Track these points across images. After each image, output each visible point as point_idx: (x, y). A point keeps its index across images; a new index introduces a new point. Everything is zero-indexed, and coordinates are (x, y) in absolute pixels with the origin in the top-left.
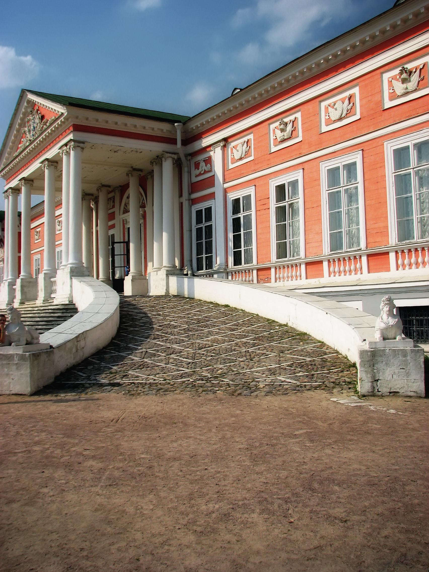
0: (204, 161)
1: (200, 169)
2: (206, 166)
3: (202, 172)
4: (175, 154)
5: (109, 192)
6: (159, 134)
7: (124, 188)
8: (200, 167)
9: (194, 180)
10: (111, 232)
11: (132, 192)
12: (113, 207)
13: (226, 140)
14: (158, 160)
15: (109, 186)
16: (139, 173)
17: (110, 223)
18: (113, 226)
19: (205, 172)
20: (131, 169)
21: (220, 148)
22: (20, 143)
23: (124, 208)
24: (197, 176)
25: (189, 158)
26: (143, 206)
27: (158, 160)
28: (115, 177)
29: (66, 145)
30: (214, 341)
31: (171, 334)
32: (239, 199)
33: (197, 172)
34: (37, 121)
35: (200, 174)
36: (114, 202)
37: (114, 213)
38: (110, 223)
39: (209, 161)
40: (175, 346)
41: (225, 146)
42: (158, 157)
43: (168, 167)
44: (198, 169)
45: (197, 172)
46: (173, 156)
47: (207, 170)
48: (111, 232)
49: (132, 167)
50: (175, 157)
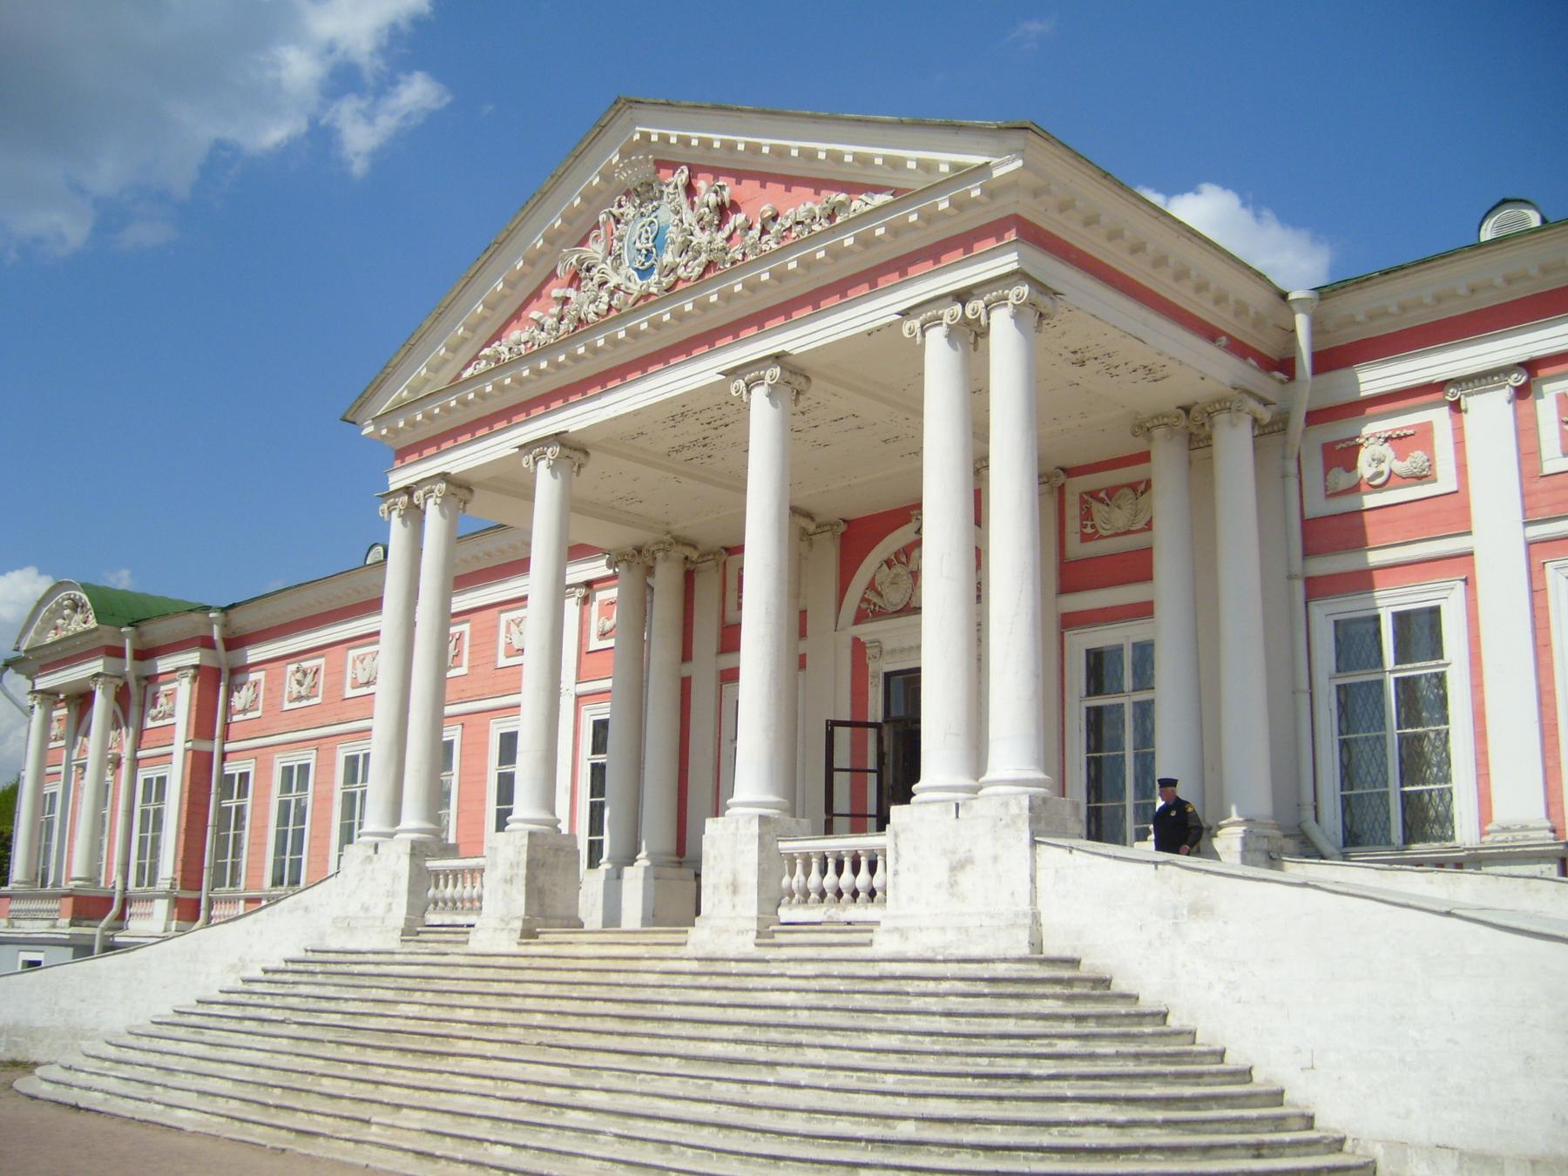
0: (1387, 440)
13: (1531, 366)
21: (1507, 393)
50: (1266, 415)
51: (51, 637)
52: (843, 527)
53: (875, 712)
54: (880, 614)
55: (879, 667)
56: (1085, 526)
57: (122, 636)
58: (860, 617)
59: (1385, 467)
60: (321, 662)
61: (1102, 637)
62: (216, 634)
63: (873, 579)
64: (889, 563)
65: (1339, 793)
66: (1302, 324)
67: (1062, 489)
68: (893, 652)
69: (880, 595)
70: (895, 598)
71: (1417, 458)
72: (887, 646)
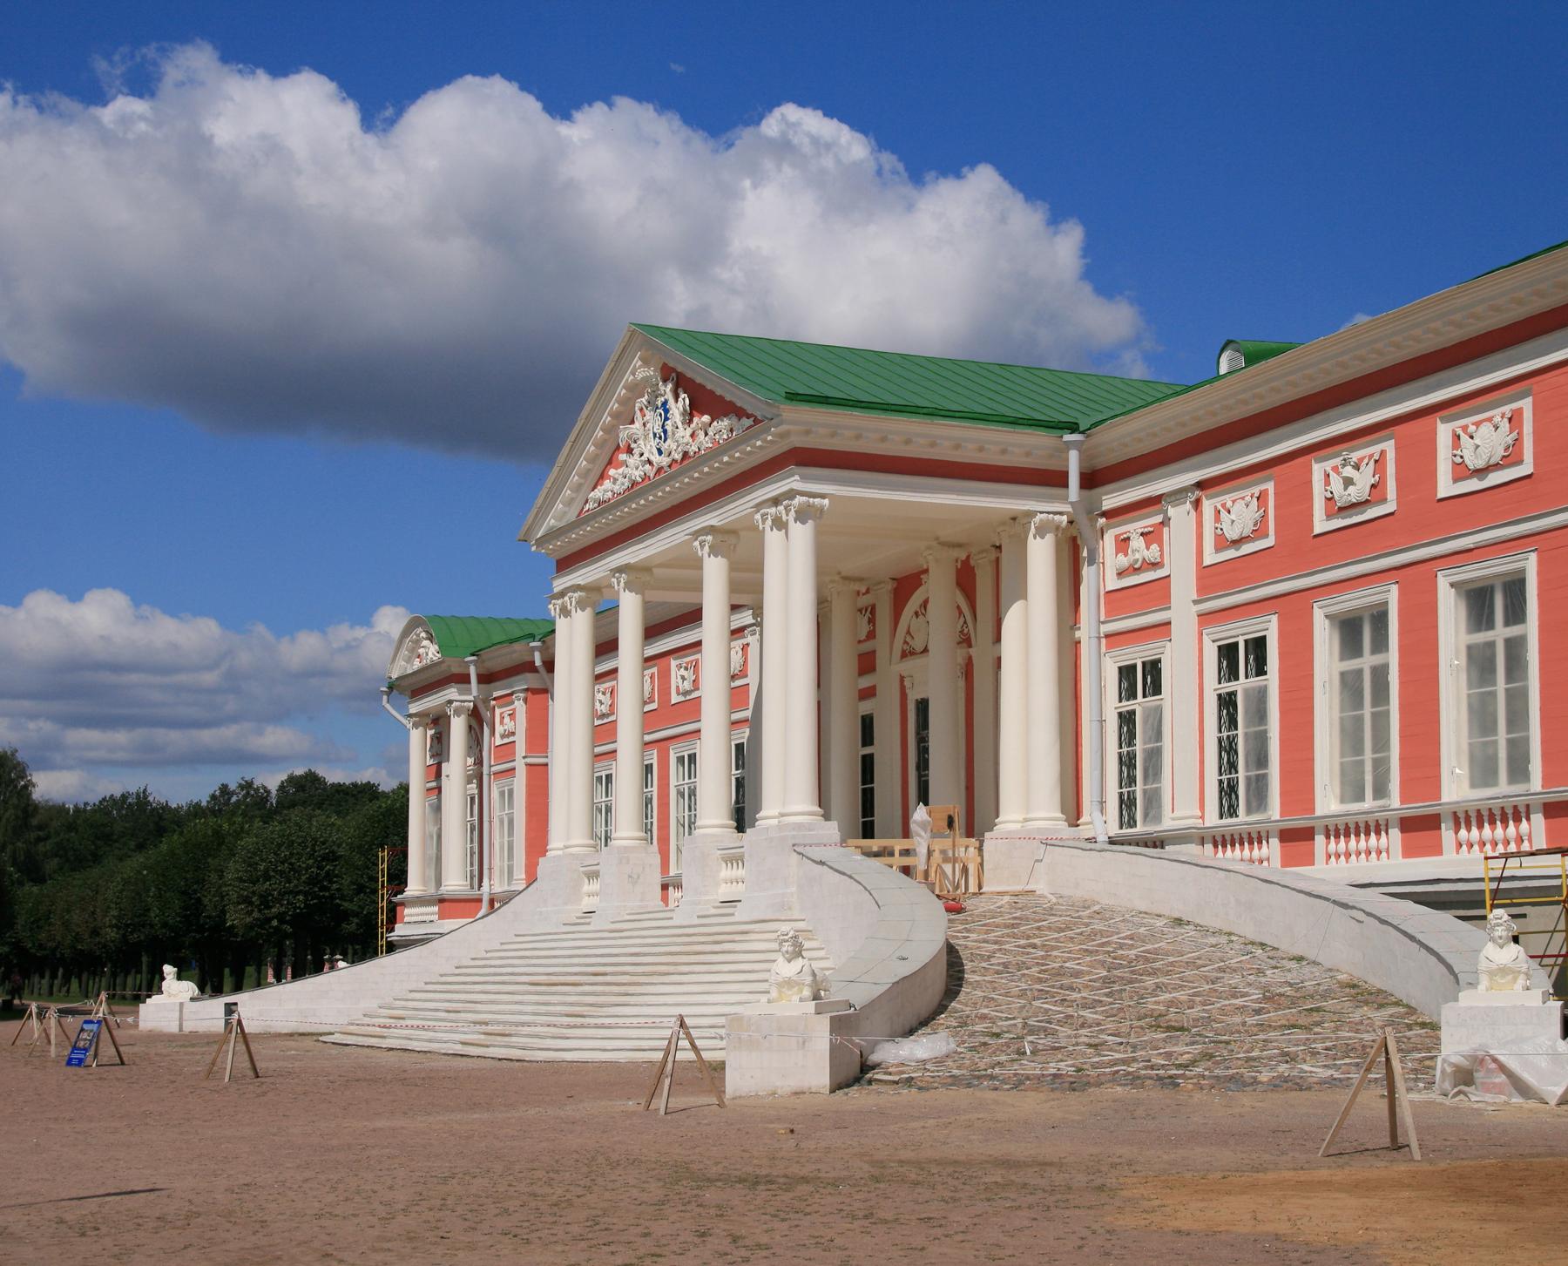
7: (906, 585)
9: (1113, 583)
10: (866, 707)
12: (871, 635)
15: (861, 580)
17: (865, 682)
18: (867, 694)
20: (934, 544)
23: (906, 642)
24: (1121, 574)
26: (966, 641)
28: (886, 558)
29: (776, 501)
30: (1171, 1003)
31: (1072, 989)
33: (1124, 561)
36: (872, 621)
38: (865, 682)
40: (1086, 1013)
41: (1197, 504)
42: (1014, 519)
48: (866, 707)
49: (937, 538)
51: (417, 665)
52: (890, 586)
54: (912, 653)
55: (913, 696)
57: (467, 664)
58: (904, 655)
62: (538, 663)
71: (1154, 547)
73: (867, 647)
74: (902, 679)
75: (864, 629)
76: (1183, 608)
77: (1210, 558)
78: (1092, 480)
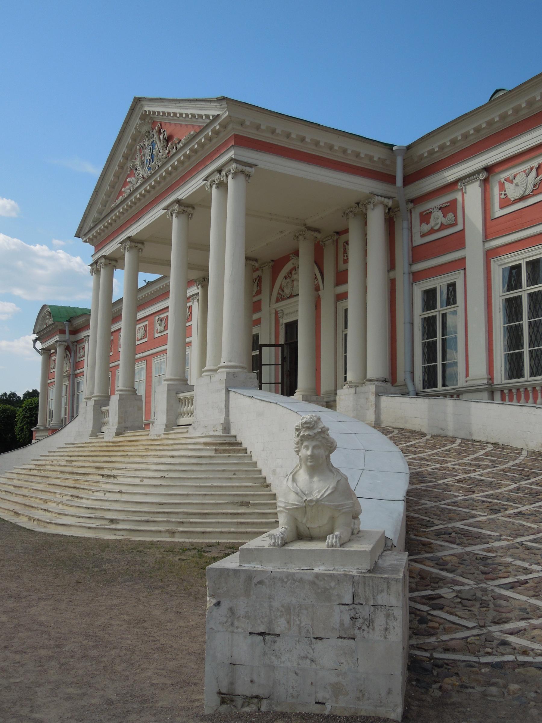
0: (440, 209)
1: (432, 223)
2: (445, 216)
3: (436, 228)
4: (389, 198)
5: (255, 270)
6: (364, 164)
8: (432, 219)
9: (418, 241)
11: (304, 264)
12: (259, 292)
13: (488, 169)
14: (359, 209)
16: (316, 234)
17: (255, 317)
18: (258, 322)
19: (443, 227)
20: (303, 228)
22: (124, 186)
23: (279, 294)
24: (423, 236)
25: (411, 205)
26: (317, 289)
27: (359, 209)
32: (519, 267)
33: (426, 228)
34: (159, 145)
35: (432, 231)
36: (259, 285)
37: (260, 301)
38: (255, 317)
39: (450, 208)
41: (486, 181)
42: (358, 204)
43: (376, 219)
44: (428, 223)
45: (426, 228)
46: (386, 200)
47: (445, 221)
49: (305, 225)
52: (271, 264)
53: (282, 341)
56: (344, 256)
58: (277, 301)
59: (439, 221)
60: (146, 323)
61: (428, 284)
63: (281, 285)
64: (286, 278)
65: (422, 366)
66: (399, 161)
67: (337, 240)
68: (287, 314)
69: (283, 291)
70: (287, 292)
71: (450, 215)
72: (285, 312)
73: (256, 299)
74: (276, 313)
75: (256, 289)
76: (473, 251)
77: (498, 212)
78: (408, 180)
